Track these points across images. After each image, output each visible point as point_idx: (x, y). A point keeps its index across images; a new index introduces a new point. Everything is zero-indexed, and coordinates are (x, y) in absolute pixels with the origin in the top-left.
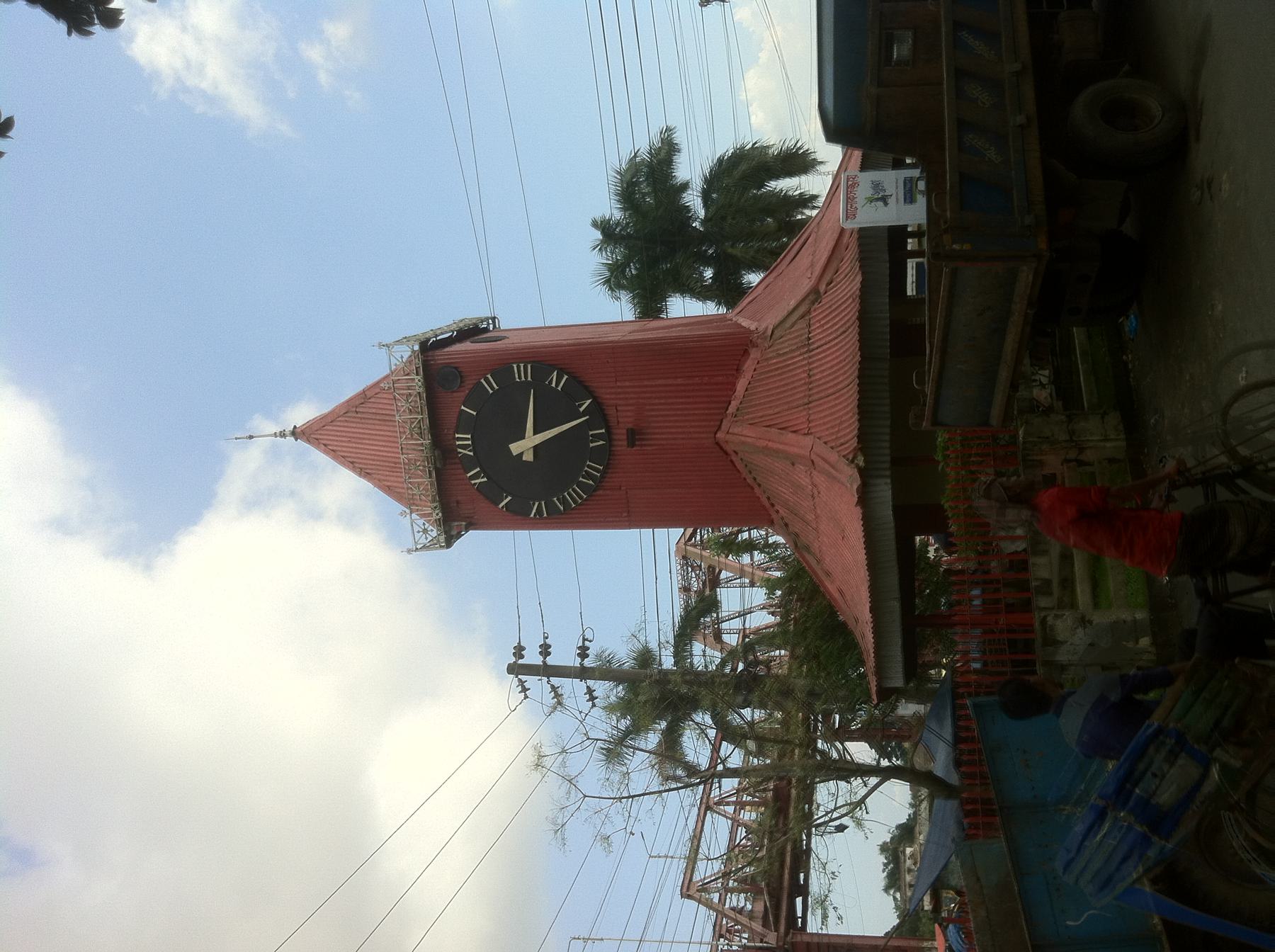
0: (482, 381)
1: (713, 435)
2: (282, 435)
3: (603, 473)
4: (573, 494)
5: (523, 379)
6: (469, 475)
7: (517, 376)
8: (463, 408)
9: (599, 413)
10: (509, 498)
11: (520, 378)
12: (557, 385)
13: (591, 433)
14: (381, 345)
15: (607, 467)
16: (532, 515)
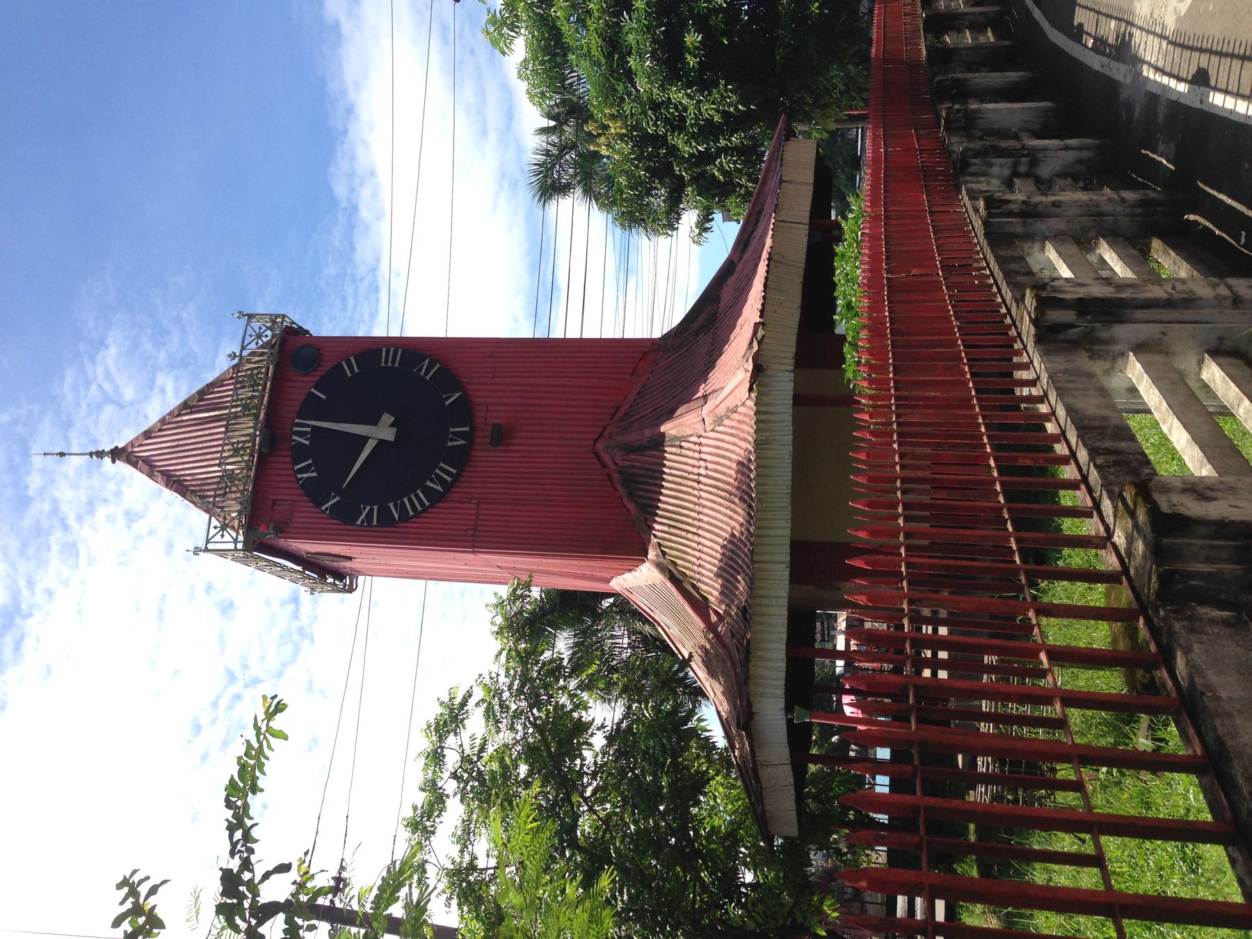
0: (344, 363)
1: (593, 442)
3: (456, 478)
5: (390, 364)
6: (296, 468)
7: (383, 360)
8: (313, 390)
10: (338, 498)
11: (386, 362)
12: (426, 374)
13: (452, 430)
14: (242, 314)
15: (461, 470)
16: (359, 522)
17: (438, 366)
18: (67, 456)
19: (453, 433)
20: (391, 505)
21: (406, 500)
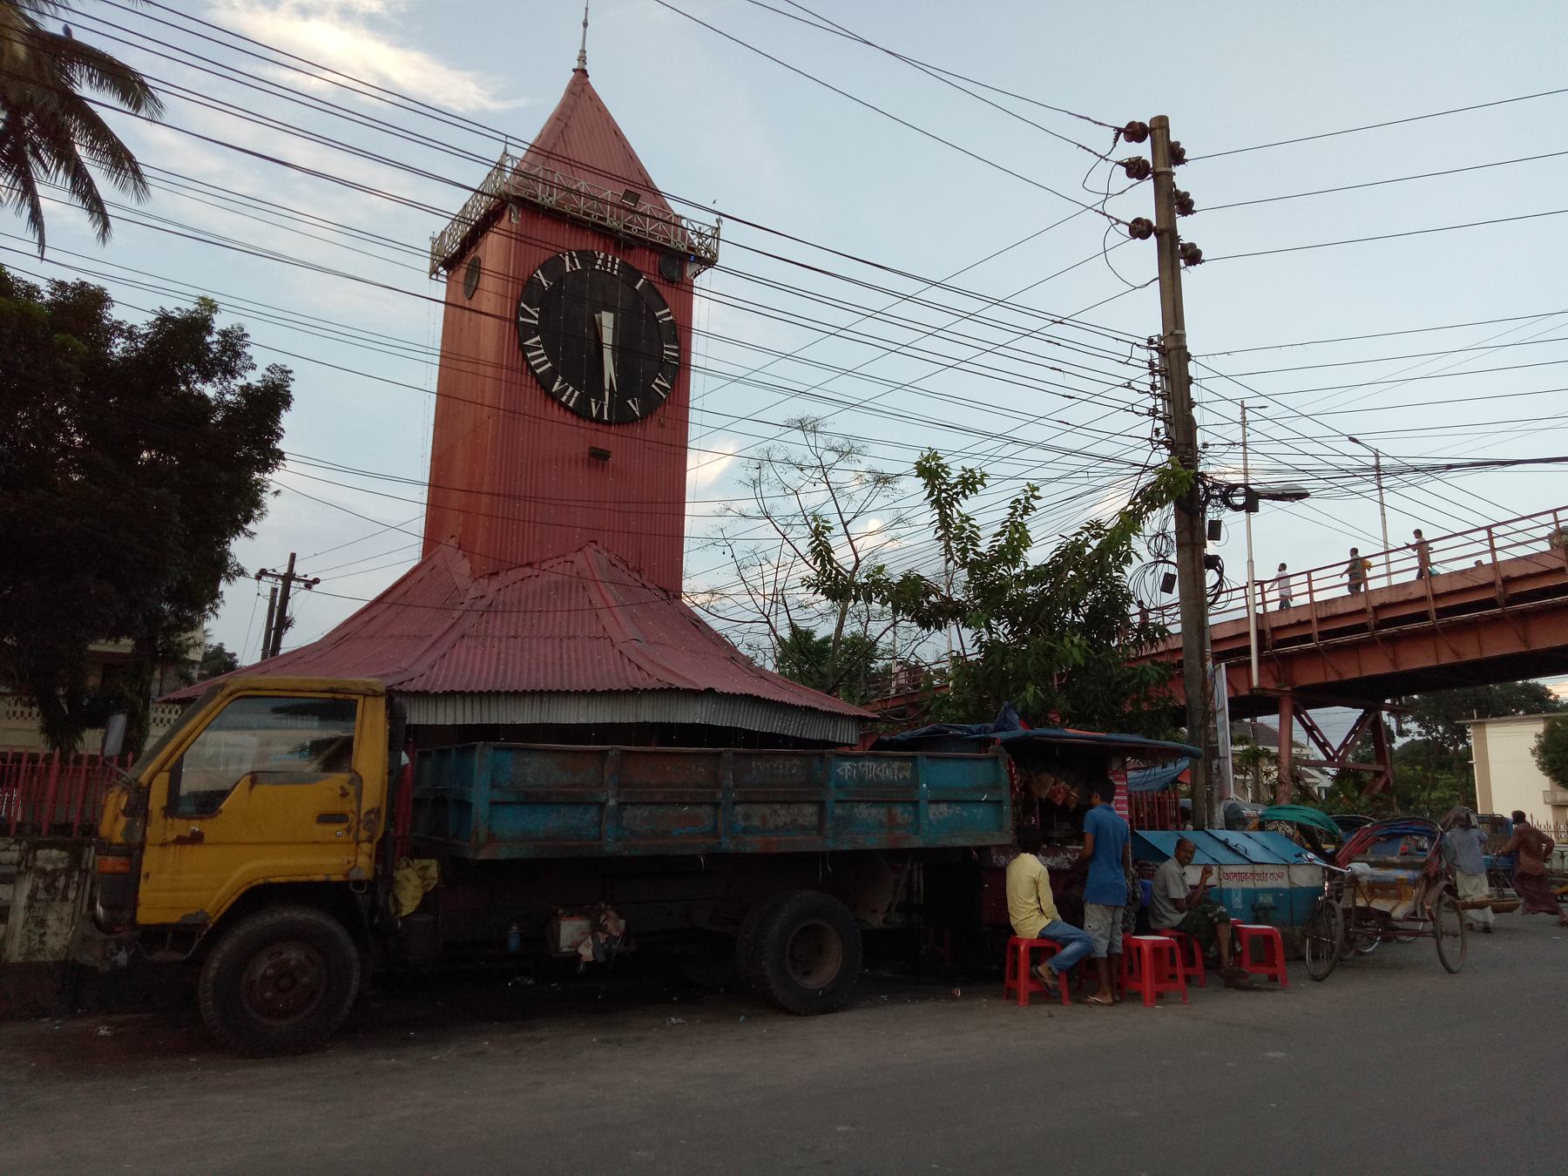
0: (668, 310)
2: (582, 58)
4: (541, 361)
9: (622, 418)
12: (656, 384)
17: (664, 396)
18: (582, 28)
21: (542, 351)
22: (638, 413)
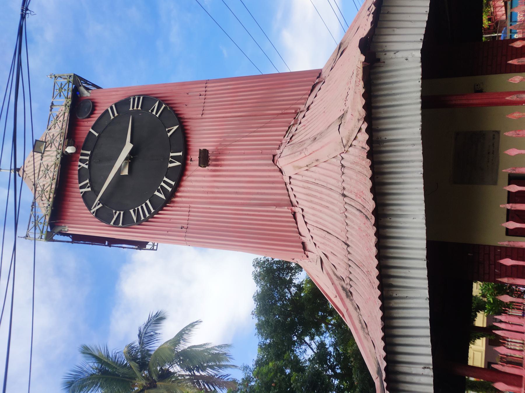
5: (135, 108)
12: (156, 113)
13: (171, 154)
17: (164, 106)
19: (172, 157)
20: (132, 211)
22: (175, 128)
